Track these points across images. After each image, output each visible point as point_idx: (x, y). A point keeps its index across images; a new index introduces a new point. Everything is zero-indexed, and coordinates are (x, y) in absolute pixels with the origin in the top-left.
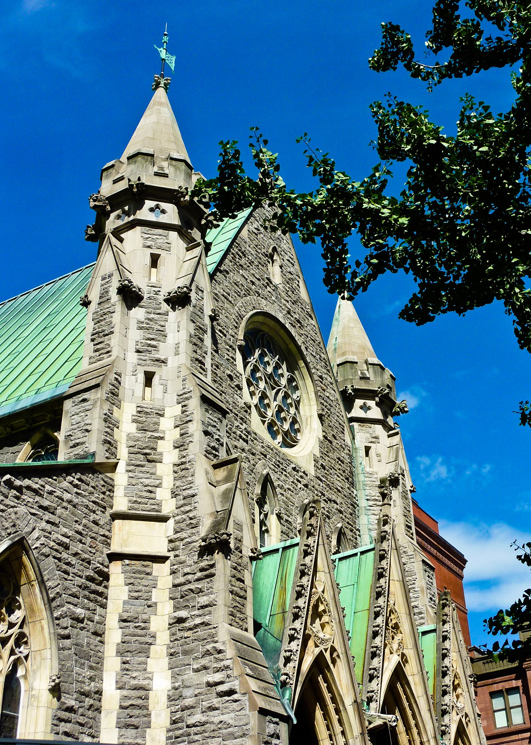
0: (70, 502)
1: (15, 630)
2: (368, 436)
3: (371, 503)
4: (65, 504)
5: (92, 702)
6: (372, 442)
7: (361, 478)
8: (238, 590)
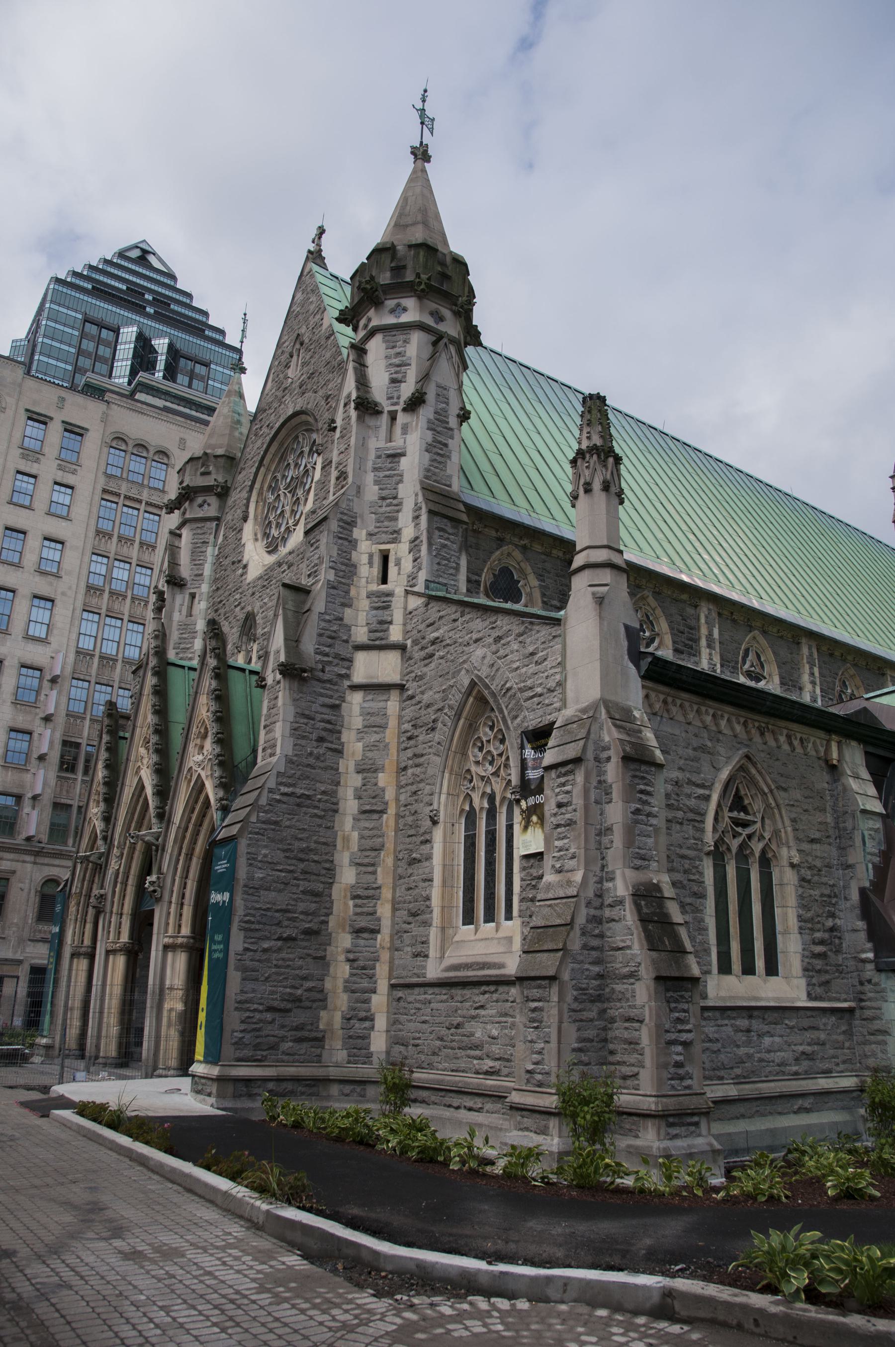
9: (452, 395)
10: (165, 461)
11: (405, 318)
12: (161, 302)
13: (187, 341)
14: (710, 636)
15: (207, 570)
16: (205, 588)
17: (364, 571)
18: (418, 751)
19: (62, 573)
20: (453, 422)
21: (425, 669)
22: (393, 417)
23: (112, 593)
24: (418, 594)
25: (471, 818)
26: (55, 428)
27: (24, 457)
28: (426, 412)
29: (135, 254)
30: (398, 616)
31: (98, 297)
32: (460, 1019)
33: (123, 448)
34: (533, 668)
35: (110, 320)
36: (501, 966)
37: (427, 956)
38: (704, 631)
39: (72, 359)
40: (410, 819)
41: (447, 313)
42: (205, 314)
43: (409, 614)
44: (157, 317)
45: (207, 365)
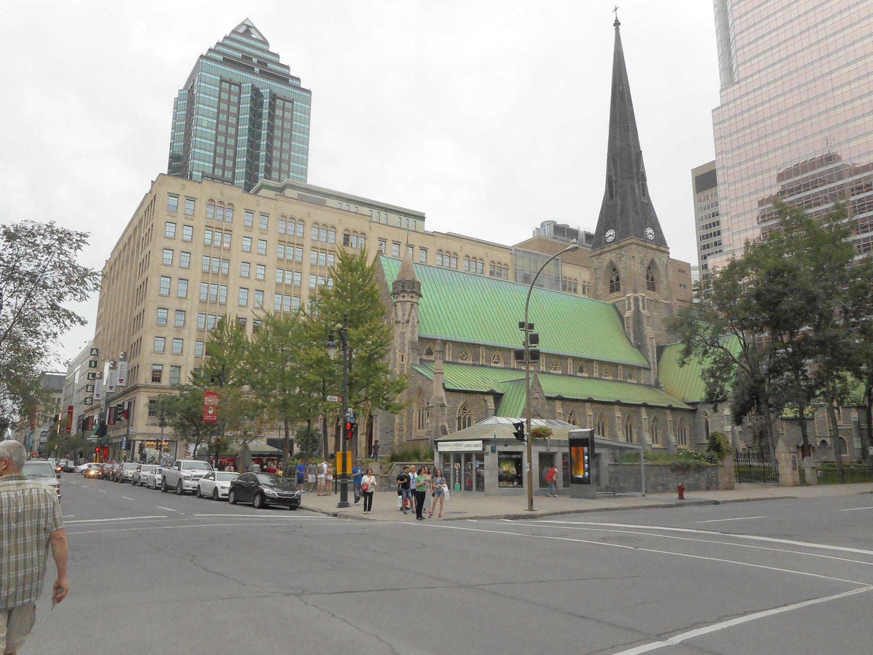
9: (416, 318)
10: (303, 223)
11: (405, 299)
12: (262, 63)
13: (279, 88)
14: (482, 355)
17: (398, 359)
19: (266, 279)
20: (416, 324)
22: (403, 323)
23: (286, 285)
26: (257, 214)
27: (246, 230)
28: (410, 323)
29: (244, 29)
30: (406, 369)
31: (225, 65)
33: (285, 220)
35: (236, 79)
38: (481, 354)
39: (216, 105)
41: (414, 295)
42: (287, 67)
43: (408, 369)
44: (263, 74)
45: (292, 102)
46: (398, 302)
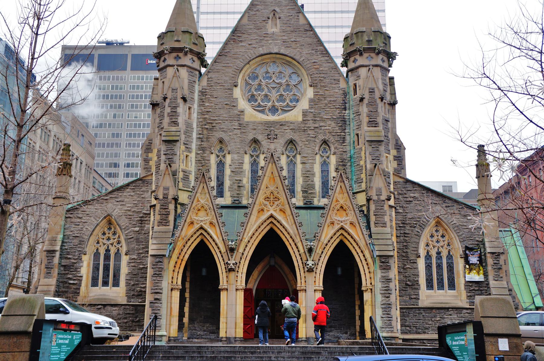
0: (130, 195)
1: (116, 240)
2: (355, 77)
3: (354, 115)
4: (128, 197)
5: (144, 255)
6: (356, 80)
7: (351, 103)
8: (164, 213)
15: (196, 96)
16: (195, 106)
18: (407, 232)
21: (408, 205)
24: (401, 177)
25: (428, 257)
32: (439, 319)
34: (465, 220)
36: (457, 304)
37: (419, 299)
40: (404, 254)
46: (377, 66)
